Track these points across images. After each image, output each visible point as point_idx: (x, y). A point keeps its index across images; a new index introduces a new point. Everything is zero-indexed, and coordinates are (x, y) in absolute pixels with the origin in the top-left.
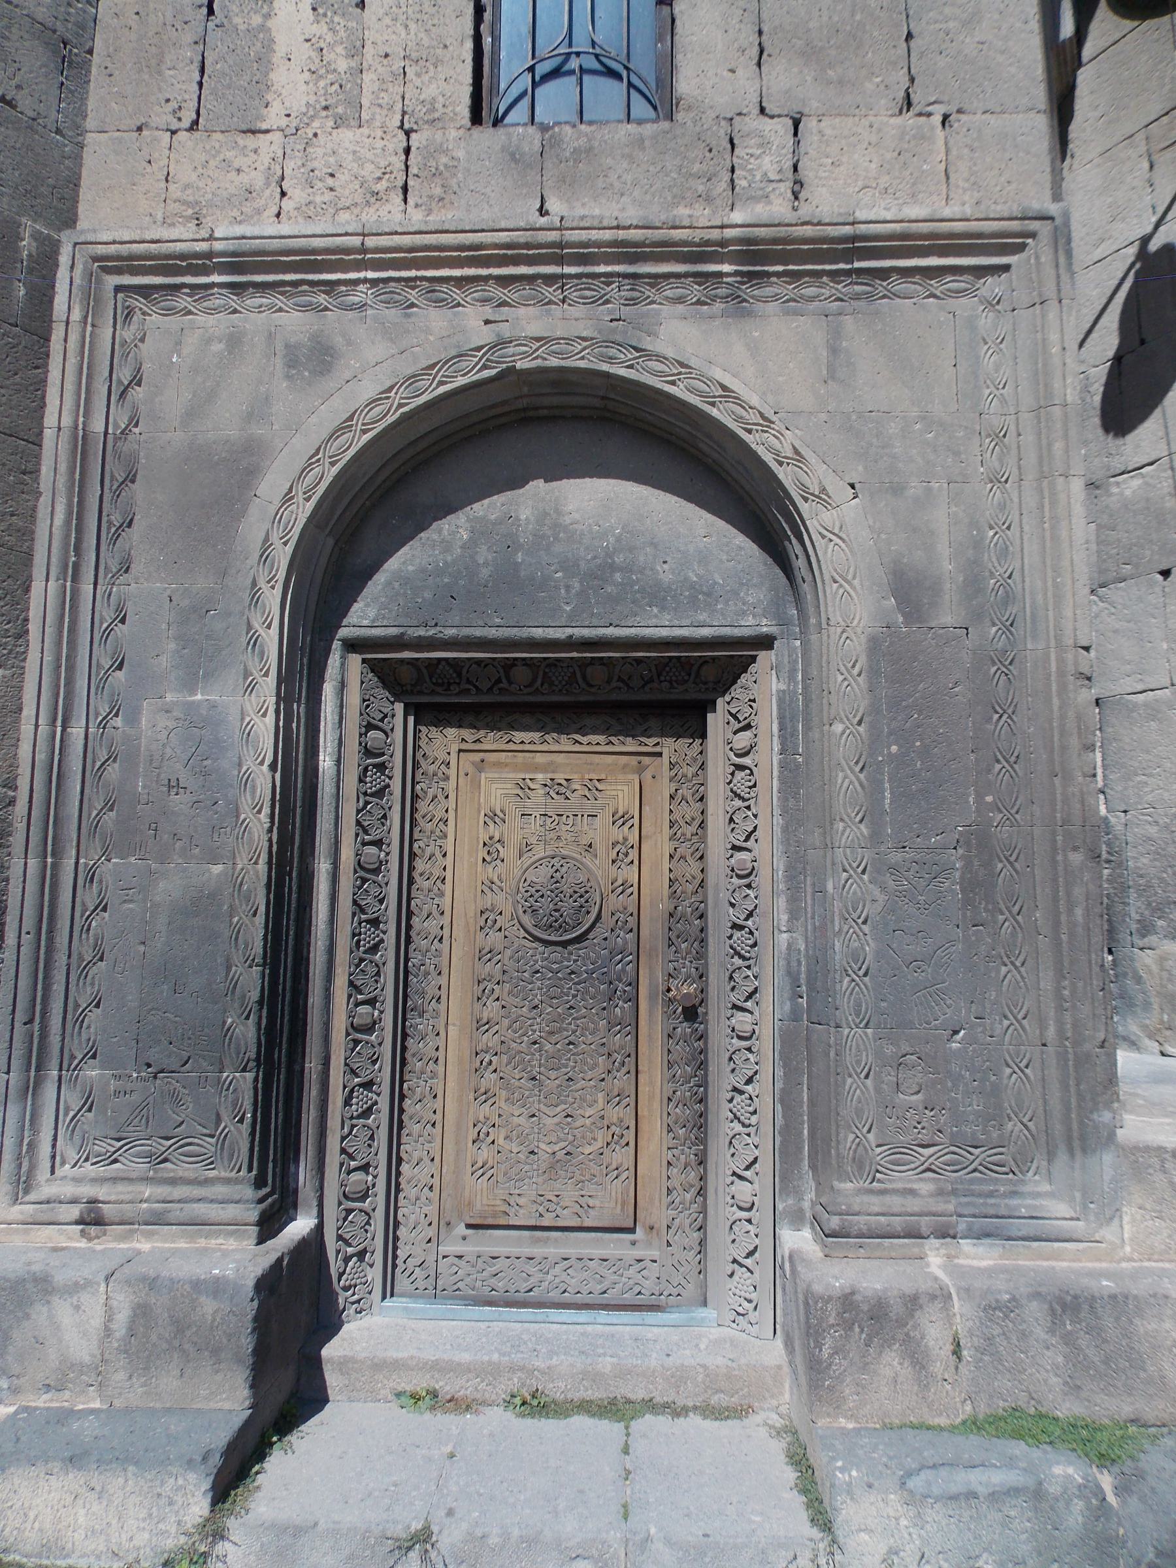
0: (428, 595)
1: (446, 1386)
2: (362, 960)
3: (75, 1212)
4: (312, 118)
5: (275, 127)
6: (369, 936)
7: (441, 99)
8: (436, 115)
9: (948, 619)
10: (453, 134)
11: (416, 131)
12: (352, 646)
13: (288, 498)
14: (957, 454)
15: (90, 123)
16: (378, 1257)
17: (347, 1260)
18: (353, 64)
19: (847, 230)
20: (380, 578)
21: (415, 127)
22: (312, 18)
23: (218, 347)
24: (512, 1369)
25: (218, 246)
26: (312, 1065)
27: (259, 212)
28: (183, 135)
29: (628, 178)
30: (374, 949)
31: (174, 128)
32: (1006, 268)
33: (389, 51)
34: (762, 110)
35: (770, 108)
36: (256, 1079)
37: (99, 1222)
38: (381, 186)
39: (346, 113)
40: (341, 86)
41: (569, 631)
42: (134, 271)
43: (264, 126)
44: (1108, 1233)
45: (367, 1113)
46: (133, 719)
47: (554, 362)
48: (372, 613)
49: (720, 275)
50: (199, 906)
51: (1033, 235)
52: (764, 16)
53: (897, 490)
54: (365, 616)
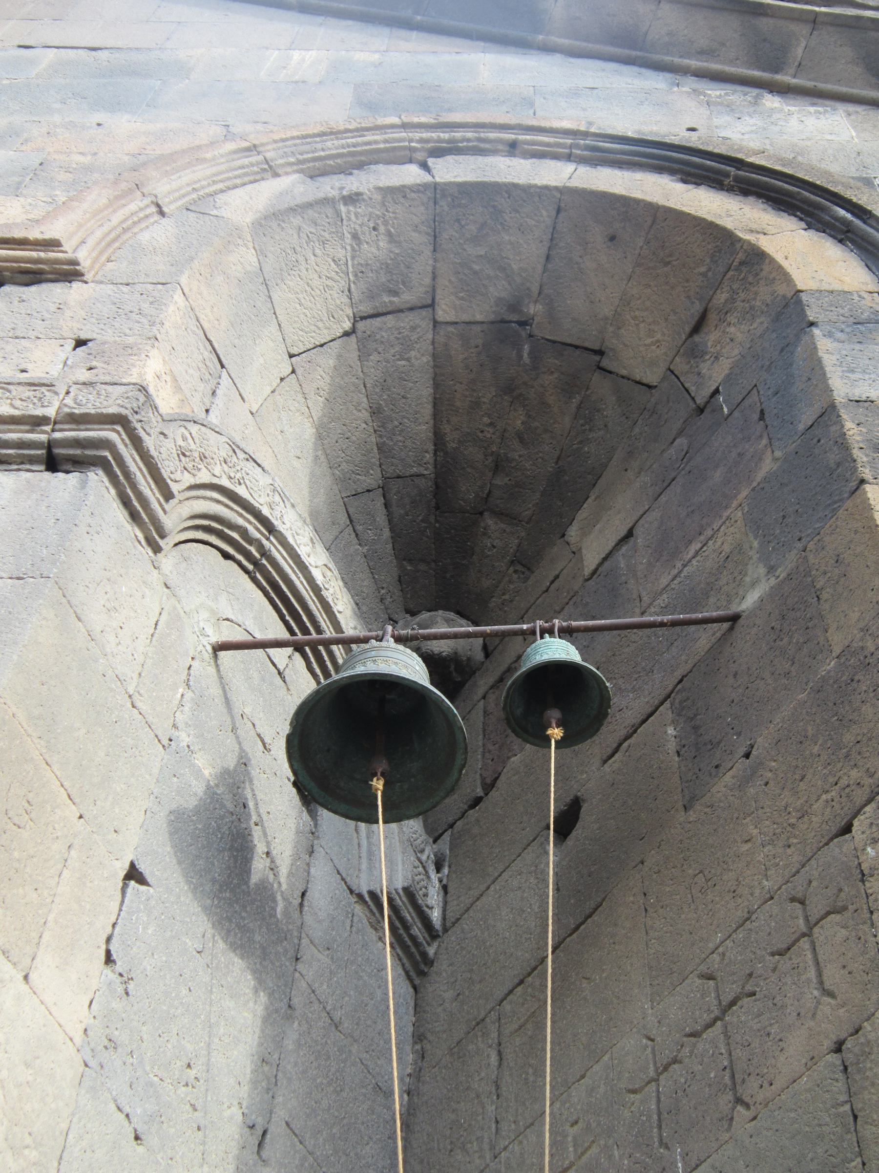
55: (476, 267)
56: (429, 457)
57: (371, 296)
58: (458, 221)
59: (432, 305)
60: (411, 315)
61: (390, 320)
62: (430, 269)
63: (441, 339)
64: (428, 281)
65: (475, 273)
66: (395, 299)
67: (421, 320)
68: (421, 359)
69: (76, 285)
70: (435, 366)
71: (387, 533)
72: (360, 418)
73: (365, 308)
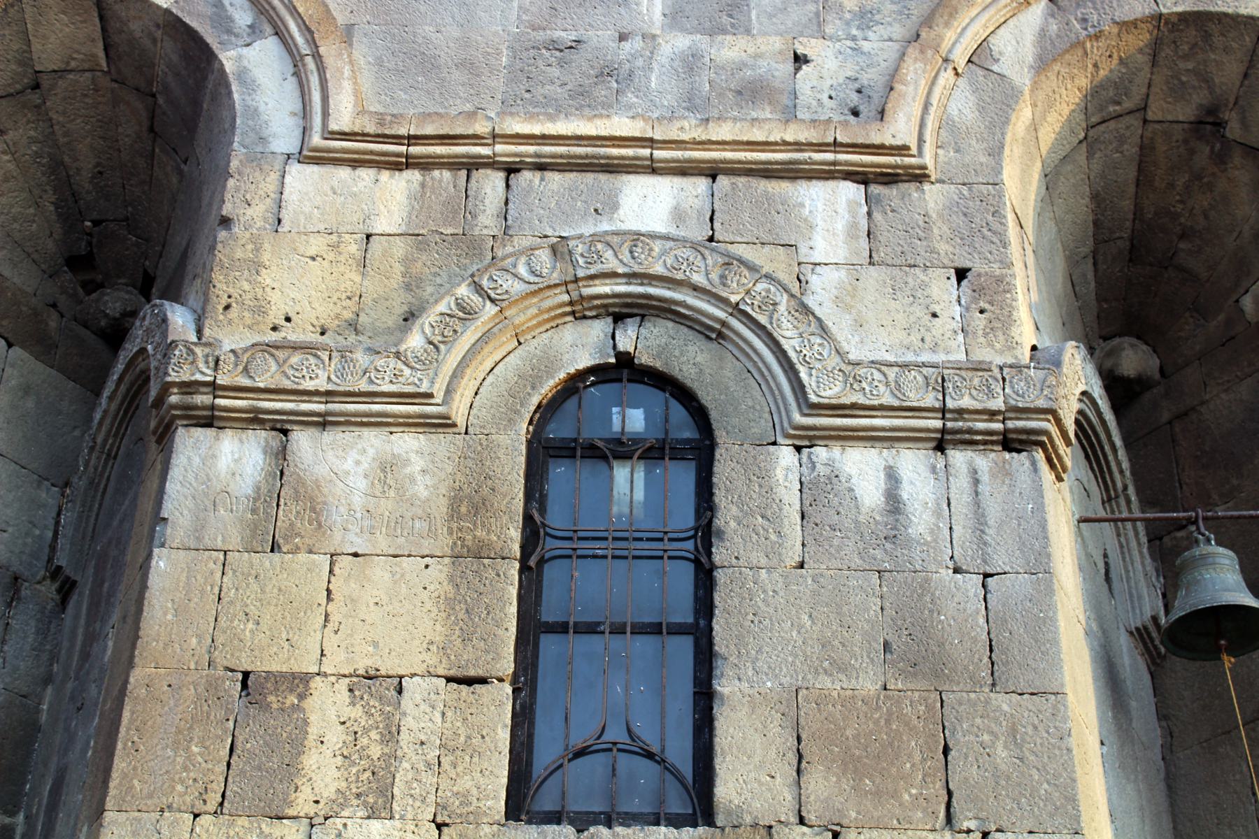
4: (342, 806)
5: (302, 814)
7: (474, 791)
8: (471, 809)
11: (447, 825)
18: (386, 750)
21: (447, 821)
22: (348, 700)
28: (205, 820)
31: (196, 811)
33: (423, 738)
34: (802, 821)
35: (811, 817)
39: (376, 803)
40: (373, 773)
43: (291, 812)
52: (802, 721)
55: (1184, 79)
56: (1128, 224)
57: (1101, 108)
58: (1174, 42)
59: (1145, 109)
60: (1127, 118)
61: (1112, 124)
62: (1147, 81)
63: (1148, 134)
64: (1144, 90)
65: (1183, 83)
66: (1117, 108)
67: (1135, 121)
68: (1131, 149)
69: (927, 187)
70: (1141, 155)
71: (1093, 284)
72: (1083, 205)
73: (1094, 120)
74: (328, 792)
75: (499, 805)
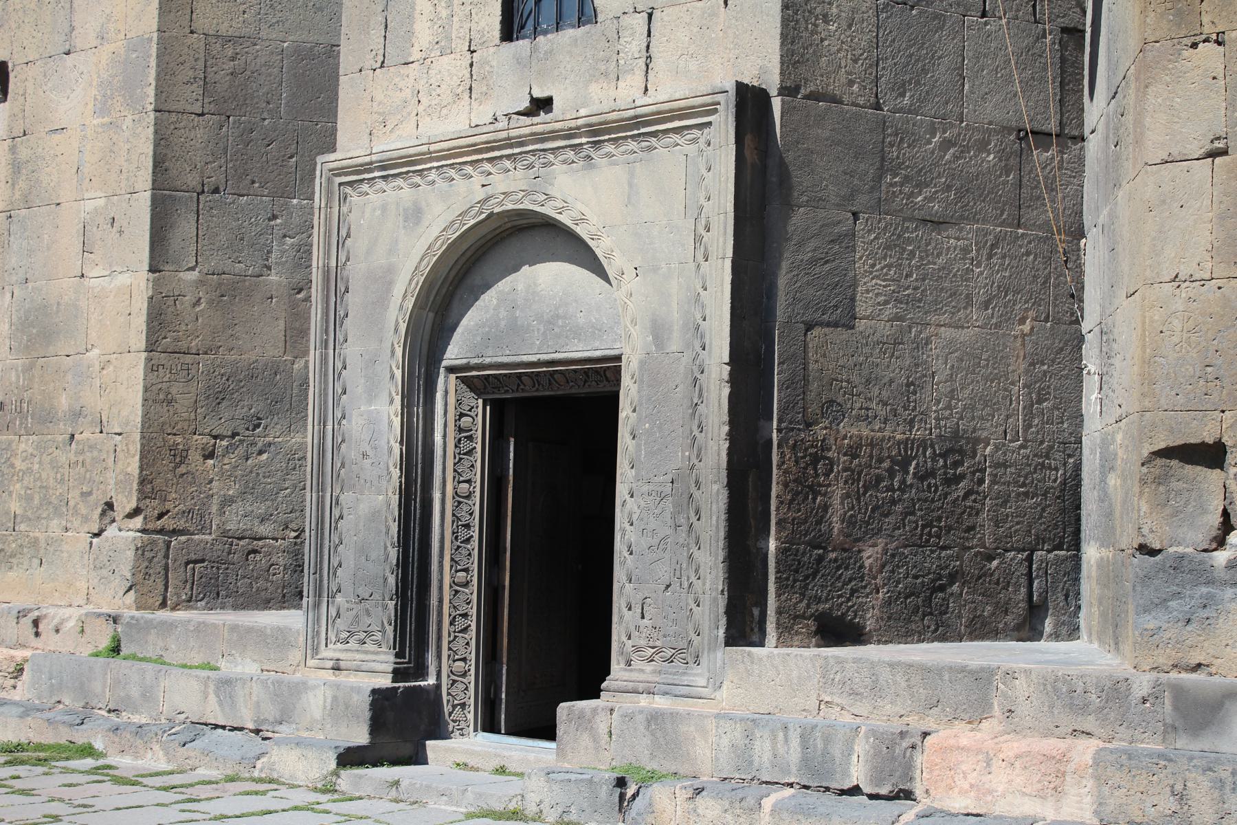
0: (479, 339)
1: (472, 762)
2: (459, 547)
3: (330, 664)
6: (463, 534)
9: (674, 348)
10: (492, 50)
12: (451, 370)
13: (405, 297)
14: (683, 245)
15: (341, 72)
16: (472, 708)
17: (454, 707)
19: (631, 113)
20: (459, 330)
23: (378, 212)
24: (496, 755)
25: (374, 158)
26: (434, 601)
27: (409, 114)
29: (569, 66)
30: (468, 541)
32: (710, 123)
36: (396, 604)
37: (338, 669)
38: (459, 91)
41: (538, 356)
42: (346, 174)
44: (718, 694)
45: (465, 630)
46: (350, 421)
47: (510, 206)
48: (456, 351)
49: (581, 144)
50: (374, 515)
51: (719, 103)
53: (655, 269)
54: (454, 353)
74: (425, 45)
75: (497, 33)
